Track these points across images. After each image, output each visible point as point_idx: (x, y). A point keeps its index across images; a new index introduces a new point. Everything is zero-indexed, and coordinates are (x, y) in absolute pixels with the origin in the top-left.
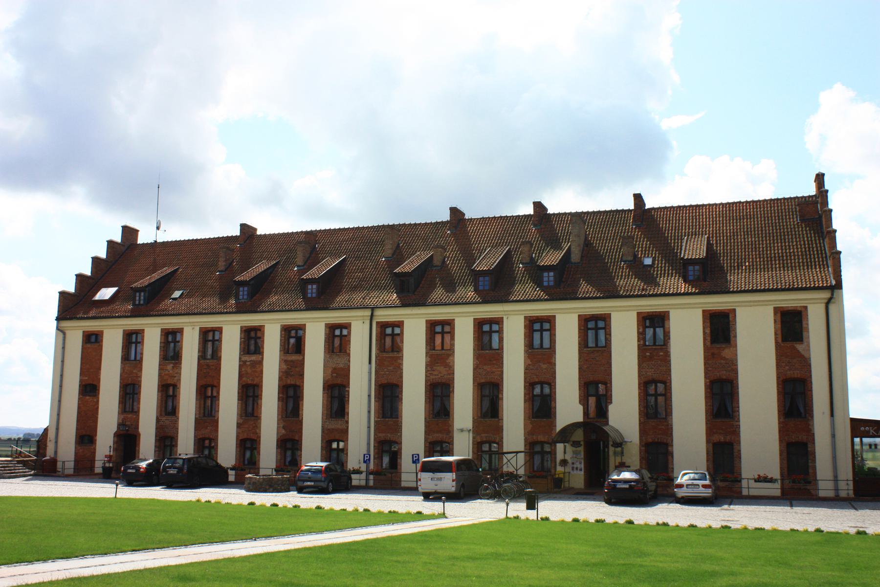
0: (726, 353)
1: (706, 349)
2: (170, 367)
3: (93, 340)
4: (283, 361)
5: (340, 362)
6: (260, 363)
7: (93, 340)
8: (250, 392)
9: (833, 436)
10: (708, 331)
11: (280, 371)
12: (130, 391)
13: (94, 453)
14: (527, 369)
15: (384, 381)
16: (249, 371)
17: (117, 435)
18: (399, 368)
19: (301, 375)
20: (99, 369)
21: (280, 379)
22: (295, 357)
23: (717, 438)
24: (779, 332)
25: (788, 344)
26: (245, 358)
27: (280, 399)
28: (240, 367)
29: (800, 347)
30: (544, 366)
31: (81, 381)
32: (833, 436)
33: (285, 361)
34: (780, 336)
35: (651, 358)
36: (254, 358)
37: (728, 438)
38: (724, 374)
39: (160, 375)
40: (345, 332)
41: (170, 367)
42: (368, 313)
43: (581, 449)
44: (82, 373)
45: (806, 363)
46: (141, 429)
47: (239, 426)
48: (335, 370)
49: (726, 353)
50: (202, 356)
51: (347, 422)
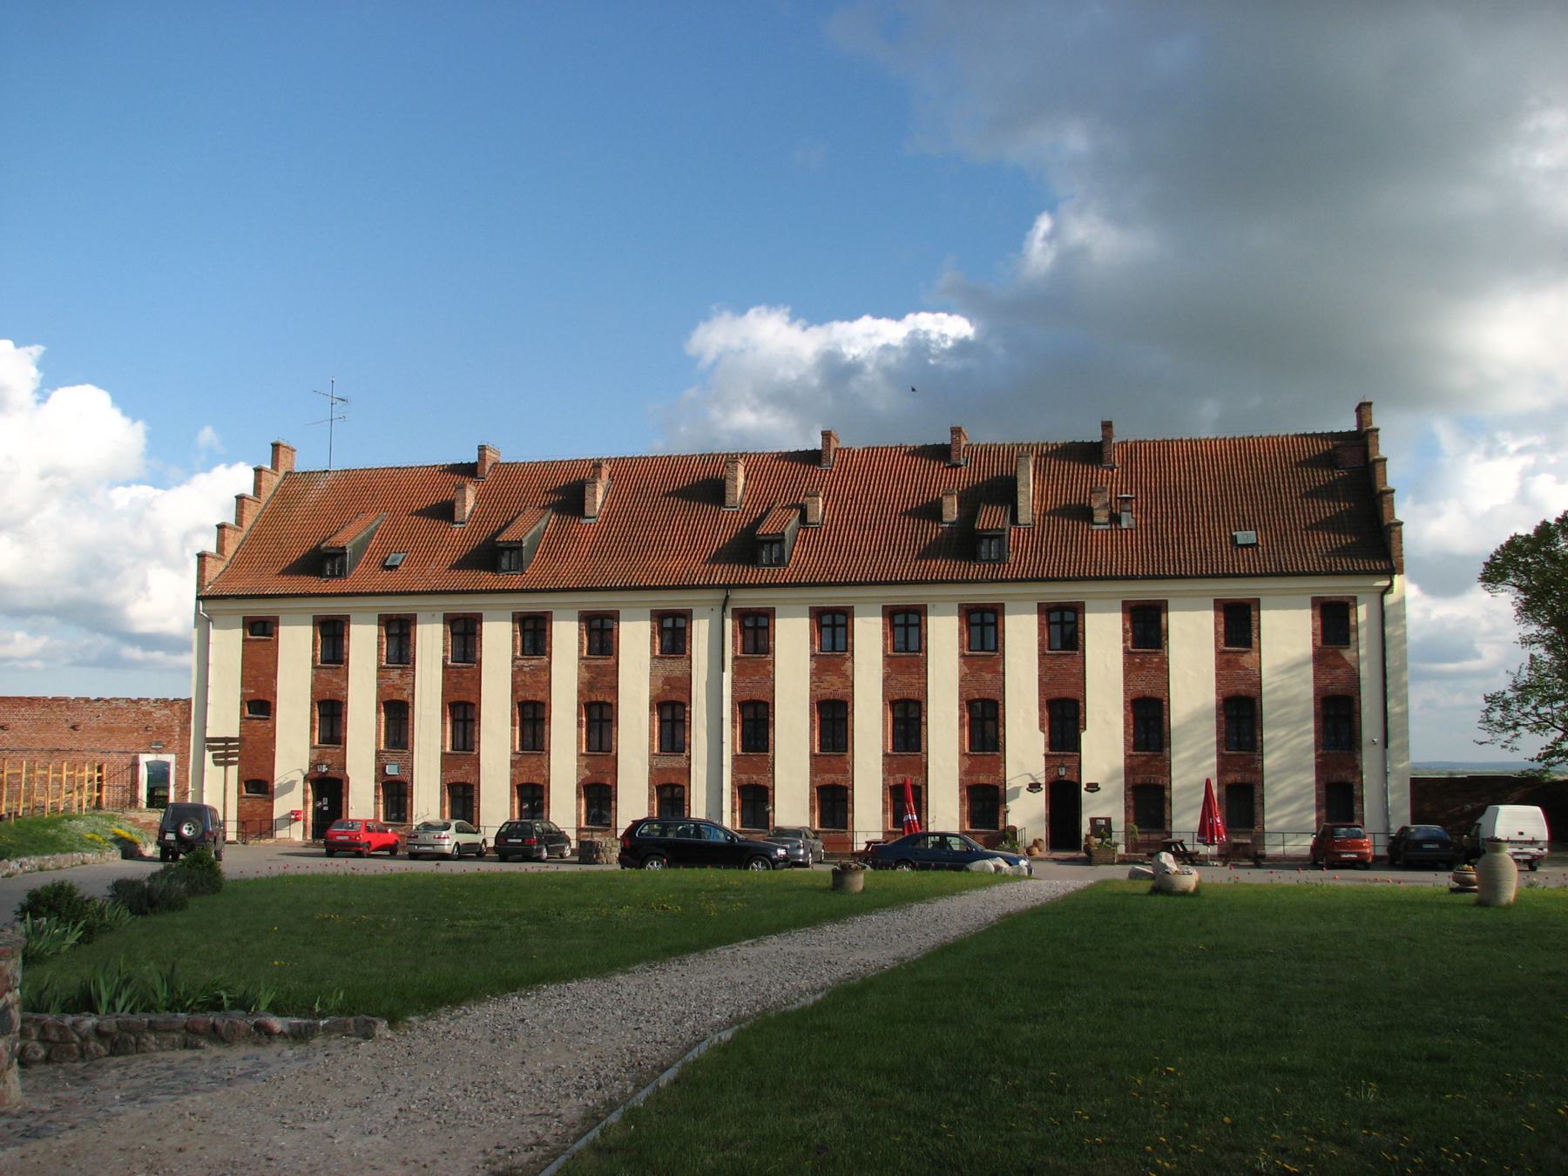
1: (1220, 653)
10: (1221, 629)
11: (580, 682)
14: (961, 680)
15: (746, 696)
16: (528, 680)
19: (614, 689)
21: (580, 692)
24: (1319, 632)
30: (988, 677)
31: (243, 694)
33: (588, 667)
34: (1319, 638)
35: (1141, 666)
37: (1248, 778)
38: (1242, 689)
39: (379, 686)
40: (681, 623)
41: (395, 674)
42: (719, 595)
44: (244, 684)
46: (350, 771)
47: (513, 764)
48: (667, 681)
49: (1246, 660)
51: (689, 758)
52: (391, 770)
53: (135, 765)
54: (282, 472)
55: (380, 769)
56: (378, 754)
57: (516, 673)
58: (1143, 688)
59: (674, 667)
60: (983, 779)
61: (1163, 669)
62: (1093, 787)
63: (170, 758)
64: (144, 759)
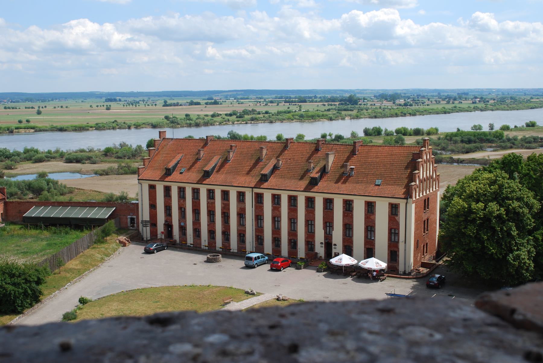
0: (372, 217)
2: (182, 201)
3: (152, 188)
4: (222, 203)
5: (242, 206)
6: (214, 203)
7: (152, 188)
8: (211, 213)
9: (405, 250)
12: (168, 209)
13: (157, 230)
14: (305, 215)
17: (165, 224)
18: (262, 210)
19: (229, 209)
20: (156, 199)
22: (226, 202)
23: (367, 246)
25: (393, 216)
26: (209, 201)
27: (222, 217)
28: (207, 204)
29: (397, 218)
32: (405, 250)
35: (347, 216)
36: (212, 201)
37: (371, 247)
42: (251, 189)
43: (323, 245)
44: (150, 200)
45: (398, 224)
46: (173, 223)
47: (208, 225)
48: (240, 208)
49: (372, 217)
50: (193, 198)
52: (182, 224)
53: (127, 219)
54: (162, 138)
55: (180, 223)
56: (179, 221)
57: (208, 203)
58: (347, 221)
59: (242, 206)
60: (310, 240)
61: (352, 217)
62: (335, 245)
63: (135, 217)
64: (129, 217)
